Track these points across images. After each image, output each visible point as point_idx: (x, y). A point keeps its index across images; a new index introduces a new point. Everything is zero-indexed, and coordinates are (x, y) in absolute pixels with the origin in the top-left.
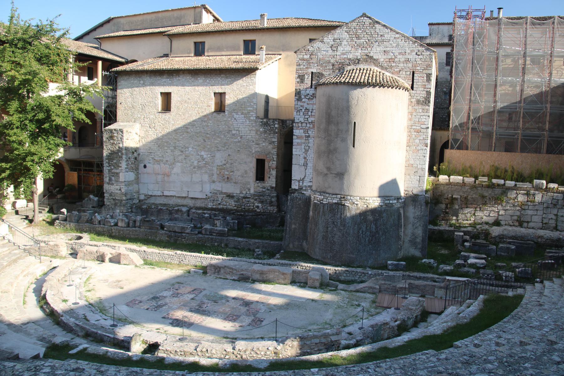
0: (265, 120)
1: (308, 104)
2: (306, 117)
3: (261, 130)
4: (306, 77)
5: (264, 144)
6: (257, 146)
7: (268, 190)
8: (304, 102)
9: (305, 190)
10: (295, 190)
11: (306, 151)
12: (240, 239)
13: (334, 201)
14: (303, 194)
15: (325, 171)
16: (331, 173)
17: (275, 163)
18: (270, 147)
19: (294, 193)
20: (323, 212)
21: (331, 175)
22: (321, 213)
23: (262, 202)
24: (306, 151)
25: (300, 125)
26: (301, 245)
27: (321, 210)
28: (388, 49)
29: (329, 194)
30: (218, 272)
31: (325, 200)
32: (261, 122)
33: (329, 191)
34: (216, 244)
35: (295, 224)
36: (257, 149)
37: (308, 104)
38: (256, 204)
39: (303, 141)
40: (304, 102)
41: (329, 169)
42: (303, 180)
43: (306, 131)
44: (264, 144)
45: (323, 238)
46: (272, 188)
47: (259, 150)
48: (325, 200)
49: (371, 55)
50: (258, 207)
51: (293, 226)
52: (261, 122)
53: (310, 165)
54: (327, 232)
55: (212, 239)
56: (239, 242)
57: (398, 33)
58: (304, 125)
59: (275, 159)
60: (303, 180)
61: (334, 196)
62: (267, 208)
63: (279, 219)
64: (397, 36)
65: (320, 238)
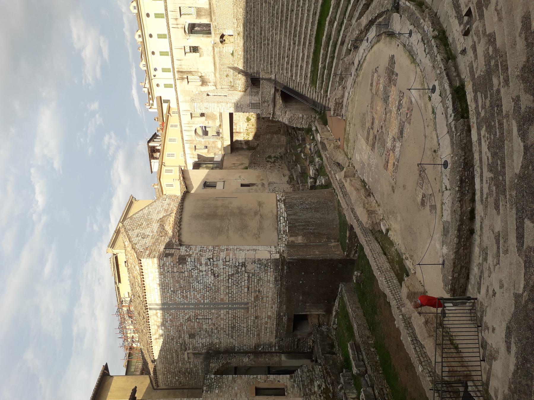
0: (205, 388)
1: (196, 250)
2: (208, 250)
3: (217, 391)
4: (168, 252)
5: (236, 388)
6: (238, 395)
7: (295, 381)
8: (193, 253)
9: (280, 250)
10: (281, 255)
11: (241, 250)
12: (355, 326)
13: (283, 206)
14: (283, 251)
15: (258, 217)
16: (259, 210)
17: (259, 376)
18: (239, 381)
19: (284, 257)
20: (294, 214)
21: (261, 210)
22: (297, 218)
23: (312, 381)
24: (241, 250)
25: (215, 254)
26: (333, 246)
27: (293, 217)
28: (156, 211)
29: (278, 211)
30: (374, 211)
31: (283, 215)
32: (207, 392)
33: (275, 211)
34: (372, 350)
35: (315, 252)
36: (243, 396)
37: (196, 250)
38: (316, 389)
39: (231, 252)
40: (193, 253)
41: (256, 213)
42: (270, 252)
43: (222, 251)
44: (236, 388)
45: (318, 212)
46: (291, 377)
47: (244, 393)
48: (283, 215)
49: (158, 219)
50: (319, 386)
51: (317, 253)
52: (207, 392)
53: (254, 247)
54: (311, 208)
55: (367, 354)
56: (359, 325)
57: (145, 208)
58: (215, 252)
59: (255, 376)
60: (270, 252)
61: (279, 207)
62: (318, 375)
63: (328, 355)
64: (147, 208)
65: (318, 215)
